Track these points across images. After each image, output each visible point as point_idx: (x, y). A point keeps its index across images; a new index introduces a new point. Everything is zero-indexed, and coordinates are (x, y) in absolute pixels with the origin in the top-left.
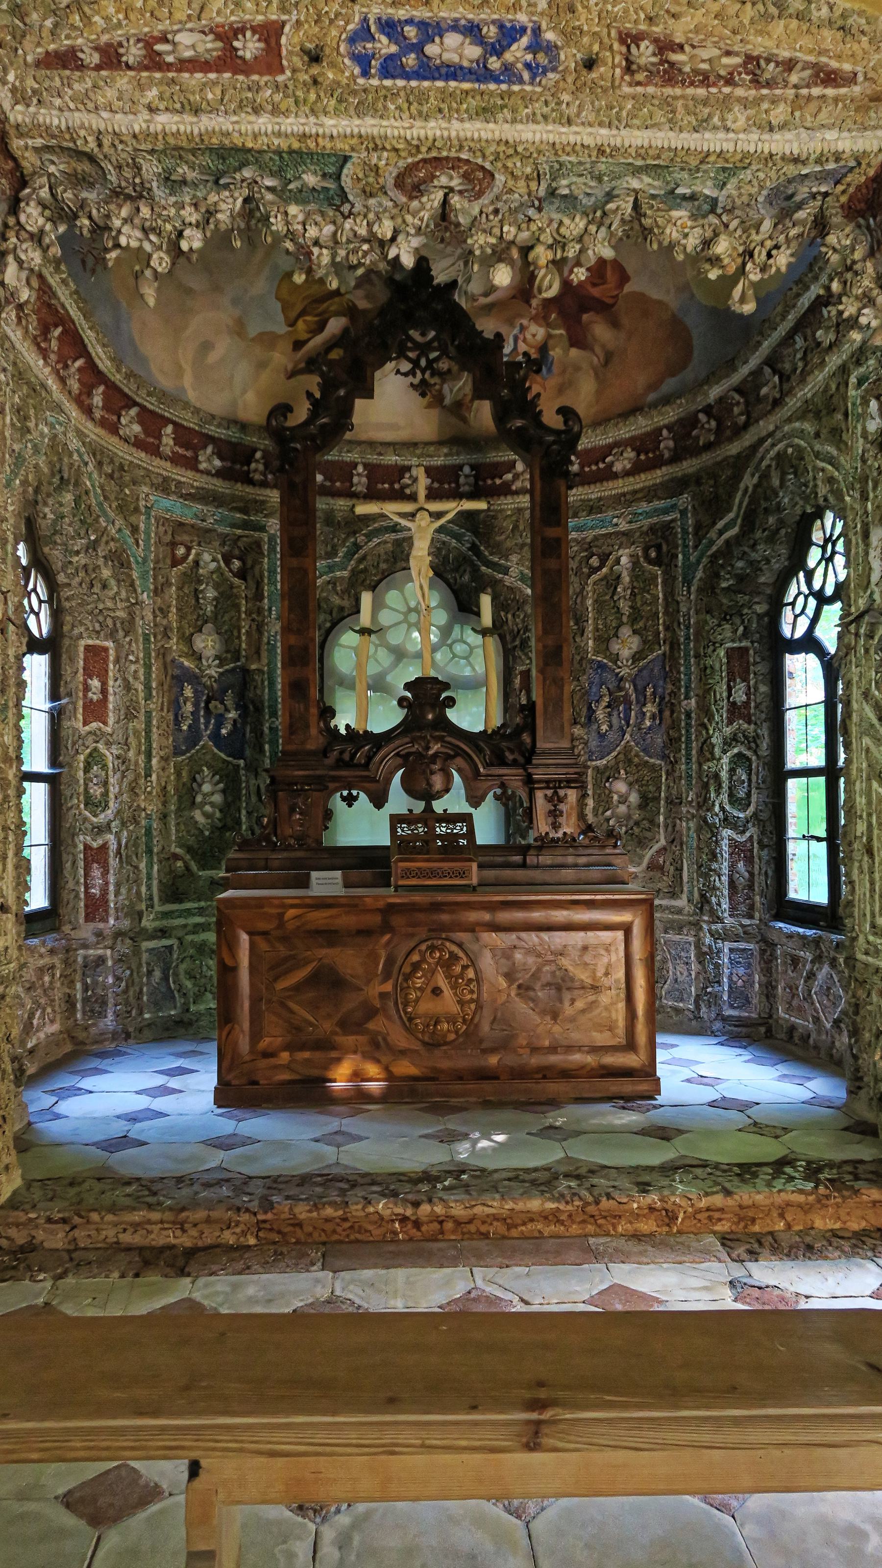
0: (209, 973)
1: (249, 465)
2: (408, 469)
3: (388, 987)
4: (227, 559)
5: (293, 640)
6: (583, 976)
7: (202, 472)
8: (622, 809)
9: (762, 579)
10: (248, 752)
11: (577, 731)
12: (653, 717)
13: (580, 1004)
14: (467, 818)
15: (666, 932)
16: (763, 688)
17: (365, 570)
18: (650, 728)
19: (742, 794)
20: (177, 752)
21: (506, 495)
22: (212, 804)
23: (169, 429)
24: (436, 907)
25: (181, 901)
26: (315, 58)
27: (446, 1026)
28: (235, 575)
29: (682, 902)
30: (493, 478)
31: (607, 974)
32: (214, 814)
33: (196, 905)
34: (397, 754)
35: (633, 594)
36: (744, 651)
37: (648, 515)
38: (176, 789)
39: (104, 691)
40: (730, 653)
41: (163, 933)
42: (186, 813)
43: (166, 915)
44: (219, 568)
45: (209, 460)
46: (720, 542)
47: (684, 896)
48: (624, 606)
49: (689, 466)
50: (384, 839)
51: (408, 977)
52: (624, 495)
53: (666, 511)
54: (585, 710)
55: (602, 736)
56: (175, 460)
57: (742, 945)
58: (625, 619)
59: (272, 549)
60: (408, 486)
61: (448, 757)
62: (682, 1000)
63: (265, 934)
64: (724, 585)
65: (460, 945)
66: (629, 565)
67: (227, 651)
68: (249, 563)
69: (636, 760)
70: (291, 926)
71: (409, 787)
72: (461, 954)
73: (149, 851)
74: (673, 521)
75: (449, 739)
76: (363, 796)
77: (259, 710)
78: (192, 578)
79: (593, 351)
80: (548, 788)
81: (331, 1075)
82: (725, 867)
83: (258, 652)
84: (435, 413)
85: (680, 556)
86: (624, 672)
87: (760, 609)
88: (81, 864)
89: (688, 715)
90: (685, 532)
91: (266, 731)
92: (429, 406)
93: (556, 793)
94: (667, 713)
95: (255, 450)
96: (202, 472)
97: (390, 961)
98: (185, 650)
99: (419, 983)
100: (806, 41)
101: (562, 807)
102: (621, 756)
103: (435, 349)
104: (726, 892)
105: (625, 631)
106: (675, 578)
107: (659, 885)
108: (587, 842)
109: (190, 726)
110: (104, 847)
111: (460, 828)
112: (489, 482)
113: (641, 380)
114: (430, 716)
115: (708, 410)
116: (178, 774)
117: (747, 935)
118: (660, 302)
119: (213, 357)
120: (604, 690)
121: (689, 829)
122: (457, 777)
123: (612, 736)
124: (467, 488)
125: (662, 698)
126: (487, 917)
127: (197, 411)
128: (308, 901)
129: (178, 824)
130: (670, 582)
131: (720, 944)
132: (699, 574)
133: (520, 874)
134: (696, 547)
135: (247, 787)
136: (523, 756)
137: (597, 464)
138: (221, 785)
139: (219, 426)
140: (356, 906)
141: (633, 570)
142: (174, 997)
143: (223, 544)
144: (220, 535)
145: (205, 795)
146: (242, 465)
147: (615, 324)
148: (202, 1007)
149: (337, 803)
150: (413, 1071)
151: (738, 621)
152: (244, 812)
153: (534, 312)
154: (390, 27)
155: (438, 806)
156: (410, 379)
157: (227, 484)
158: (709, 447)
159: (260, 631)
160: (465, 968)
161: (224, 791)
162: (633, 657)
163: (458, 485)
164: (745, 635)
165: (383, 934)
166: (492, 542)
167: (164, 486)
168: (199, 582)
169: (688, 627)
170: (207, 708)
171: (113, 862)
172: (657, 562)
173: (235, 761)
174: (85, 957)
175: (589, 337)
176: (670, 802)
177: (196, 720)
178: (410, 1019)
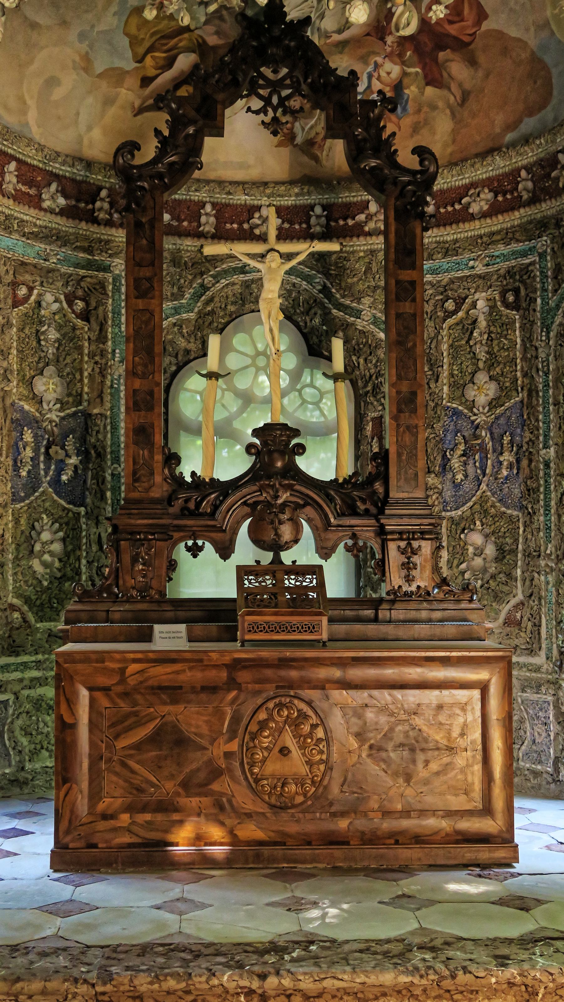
0: (46, 730)
1: (93, 204)
2: (258, 208)
3: (234, 746)
4: (70, 301)
5: (137, 384)
6: (439, 737)
7: (45, 210)
8: (478, 562)
10: (88, 500)
11: (432, 480)
12: (510, 466)
13: (434, 766)
14: (317, 571)
15: (523, 691)
17: (212, 312)
18: (507, 478)
20: (16, 499)
21: (358, 236)
22: (51, 553)
23: (13, 166)
24: (284, 663)
25: (17, 655)
27: (293, 787)
28: (77, 317)
29: (540, 660)
30: (345, 219)
31: (462, 735)
32: (53, 563)
33: (33, 658)
34: (245, 503)
35: (490, 339)
37: (506, 258)
38: (14, 537)
42: (23, 562)
44: (61, 309)
45: (53, 198)
47: (543, 653)
48: (481, 353)
50: (231, 592)
51: (254, 736)
52: (481, 237)
53: (524, 254)
54: (439, 458)
55: (457, 486)
56: (18, 197)
58: (481, 365)
59: (116, 290)
60: (257, 226)
61: (298, 507)
62: (540, 762)
63: (106, 690)
65: (309, 703)
66: (486, 309)
67: (69, 395)
68: (93, 304)
69: (493, 510)
70: (132, 681)
72: (310, 713)
74: (530, 264)
75: (298, 487)
76: (208, 546)
77: (100, 456)
79: (449, 89)
80: (401, 539)
81: (172, 838)
83: (100, 396)
84: (285, 152)
85: (539, 301)
89: (547, 465)
90: (544, 276)
91: (109, 478)
92: (279, 145)
93: (409, 544)
94: (525, 463)
95: (100, 189)
96: (45, 210)
97: (236, 719)
98: (25, 393)
99: (266, 742)
101: (416, 559)
102: (477, 507)
103: (288, 87)
105: (482, 377)
106: (533, 323)
107: (517, 642)
108: (442, 596)
109: (29, 472)
111: (310, 581)
112: (341, 222)
113: (499, 119)
114: (279, 464)
116: (17, 521)
118: (519, 40)
119: (58, 93)
120: (460, 438)
121: (548, 583)
123: (467, 486)
124: (318, 229)
125: (520, 447)
126: (337, 673)
127: (41, 148)
128: (151, 655)
129: (15, 574)
133: (371, 629)
135: (88, 536)
136: (376, 506)
137: (453, 206)
138: (61, 534)
139: (64, 163)
140: (201, 661)
141: (490, 314)
142: (8, 755)
144: (62, 275)
145: (44, 544)
146: (87, 203)
147: (472, 62)
148: (38, 766)
150: (260, 835)
152: (84, 562)
153: (389, 49)
155: (287, 557)
156: (262, 116)
157: (70, 223)
160: (314, 727)
161: (64, 540)
162: (490, 404)
163: (309, 227)
165: (229, 690)
166: (343, 284)
168: (41, 323)
169: (546, 374)
170: (47, 453)
172: (516, 306)
173: (75, 509)
175: (445, 75)
176: (527, 555)
178: (257, 781)
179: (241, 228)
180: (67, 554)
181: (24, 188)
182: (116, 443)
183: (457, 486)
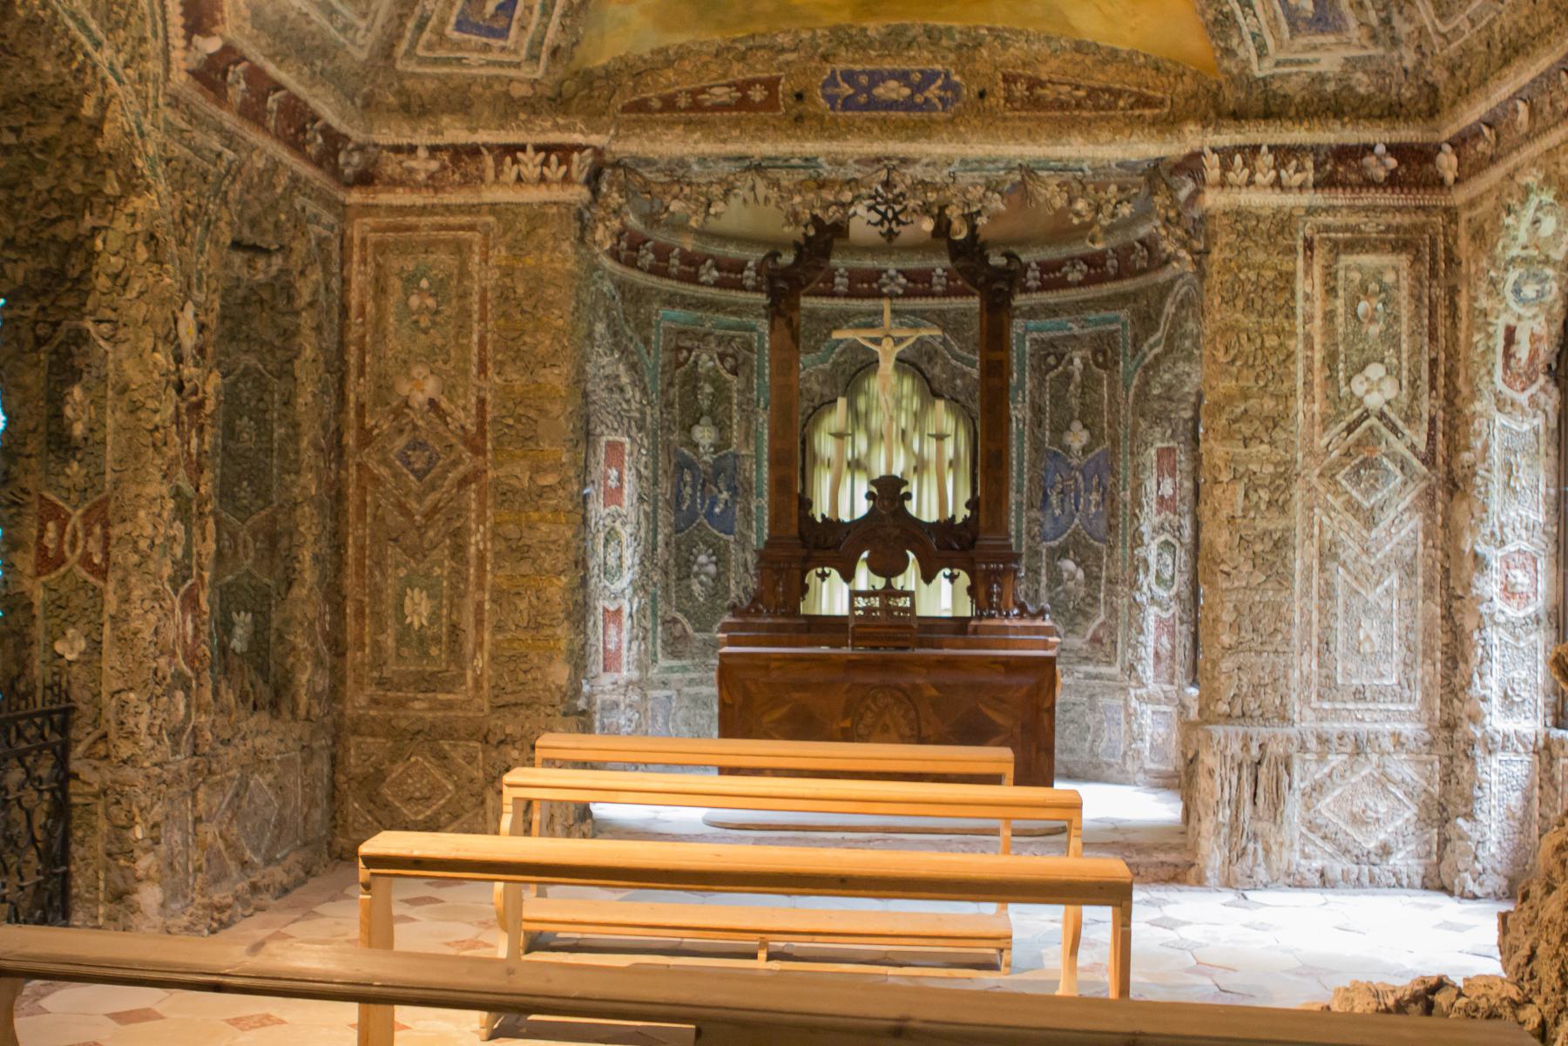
2: (886, 271)
4: (722, 357)
9: (1186, 389)
10: (738, 527)
12: (1097, 505)
16: (1188, 484)
19: (1167, 575)
22: (707, 574)
26: (799, 97)
35: (1083, 393)
36: (1171, 450)
37: (1096, 323)
39: (620, 479)
40: (1161, 453)
41: (665, 684)
42: (685, 582)
43: (671, 669)
46: (1150, 357)
47: (1118, 666)
49: (1128, 285)
53: (1111, 322)
55: (1056, 520)
57: (1163, 708)
64: (1155, 392)
71: (875, 569)
73: (654, 614)
76: (835, 574)
78: (692, 380)
82: (1151, 639)
86: (1075, 462)
87: (1188, 414)
88: (601, 624)
94: (1108, 502)
100: (1132, 77)
104: (1151, 662)
105: (1077, 426)
110: (619, 611)
115: (1142, 242)
117: (1168, 700)
122: (911, 556)
130: (1112, 385)
131: (1144, 707)
132: (1135, 382)
134: (1134, 356)
143: (719, 345)
144: (716, 337)
145: (702, 565)
149: (812, 577)
151: (1166, 424)
154: (849, 77)
156: (879, 228)
158: (1143, 271)
159: (749, 421)
163: (931, 285)
164: (1173, 436)
167: (671, 301)
170: (702, 490)
171: (626, 623)
174: (603, 702)
176: (1109, 581)
177: (694, 501)
179: (871, 288)
180: (719, 574)
181: (687, 269)
182: (759, 479)
183: (1056, 520)
